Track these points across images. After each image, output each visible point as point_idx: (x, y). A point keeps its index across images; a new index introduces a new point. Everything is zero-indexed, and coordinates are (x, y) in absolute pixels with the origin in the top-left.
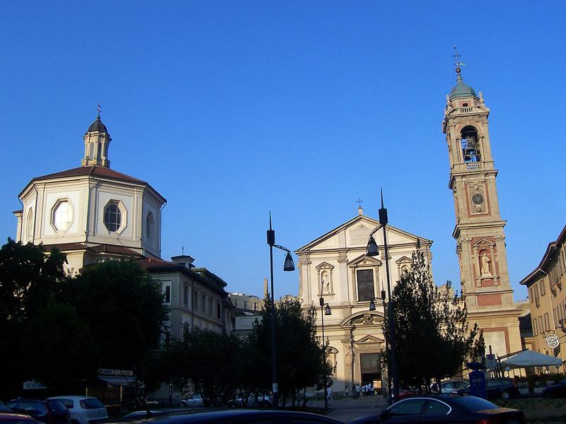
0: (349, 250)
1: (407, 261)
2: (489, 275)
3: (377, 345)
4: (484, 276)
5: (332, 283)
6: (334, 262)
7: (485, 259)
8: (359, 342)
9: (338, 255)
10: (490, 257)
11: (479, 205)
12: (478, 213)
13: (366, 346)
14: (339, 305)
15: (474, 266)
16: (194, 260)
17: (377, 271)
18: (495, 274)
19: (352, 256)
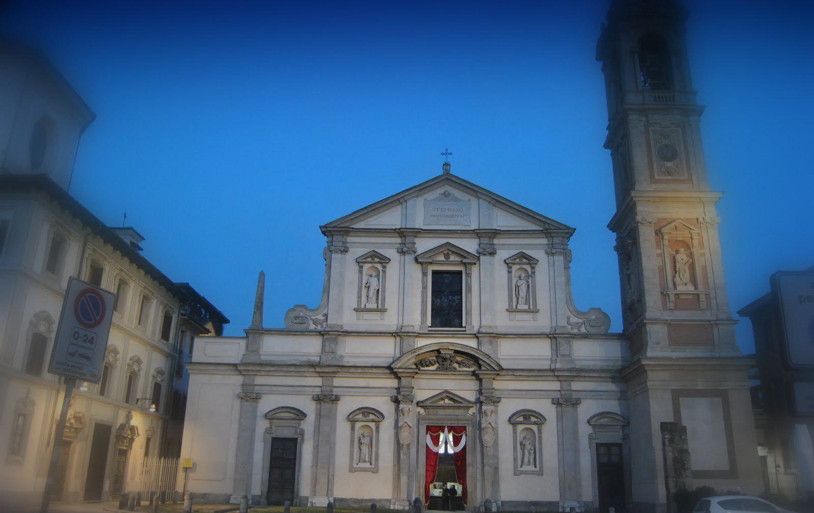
0: (418, 232)
1: (524, 260)
2: (690, 288)
3: (459, 412)
4: (680, 288)
5: (384, 291)
6: (391, 253)
7: (682, 257)
8: (428, 403)
9: (399, 240)
10: (691, 255)
11: (669, 164)
12: (669, 178)
13: (441, 412)
14: (394, 329)
15: (662, 270)
16: (143, 239)
17: (469, 275)
18: (700, 287)
19: (424, 245)
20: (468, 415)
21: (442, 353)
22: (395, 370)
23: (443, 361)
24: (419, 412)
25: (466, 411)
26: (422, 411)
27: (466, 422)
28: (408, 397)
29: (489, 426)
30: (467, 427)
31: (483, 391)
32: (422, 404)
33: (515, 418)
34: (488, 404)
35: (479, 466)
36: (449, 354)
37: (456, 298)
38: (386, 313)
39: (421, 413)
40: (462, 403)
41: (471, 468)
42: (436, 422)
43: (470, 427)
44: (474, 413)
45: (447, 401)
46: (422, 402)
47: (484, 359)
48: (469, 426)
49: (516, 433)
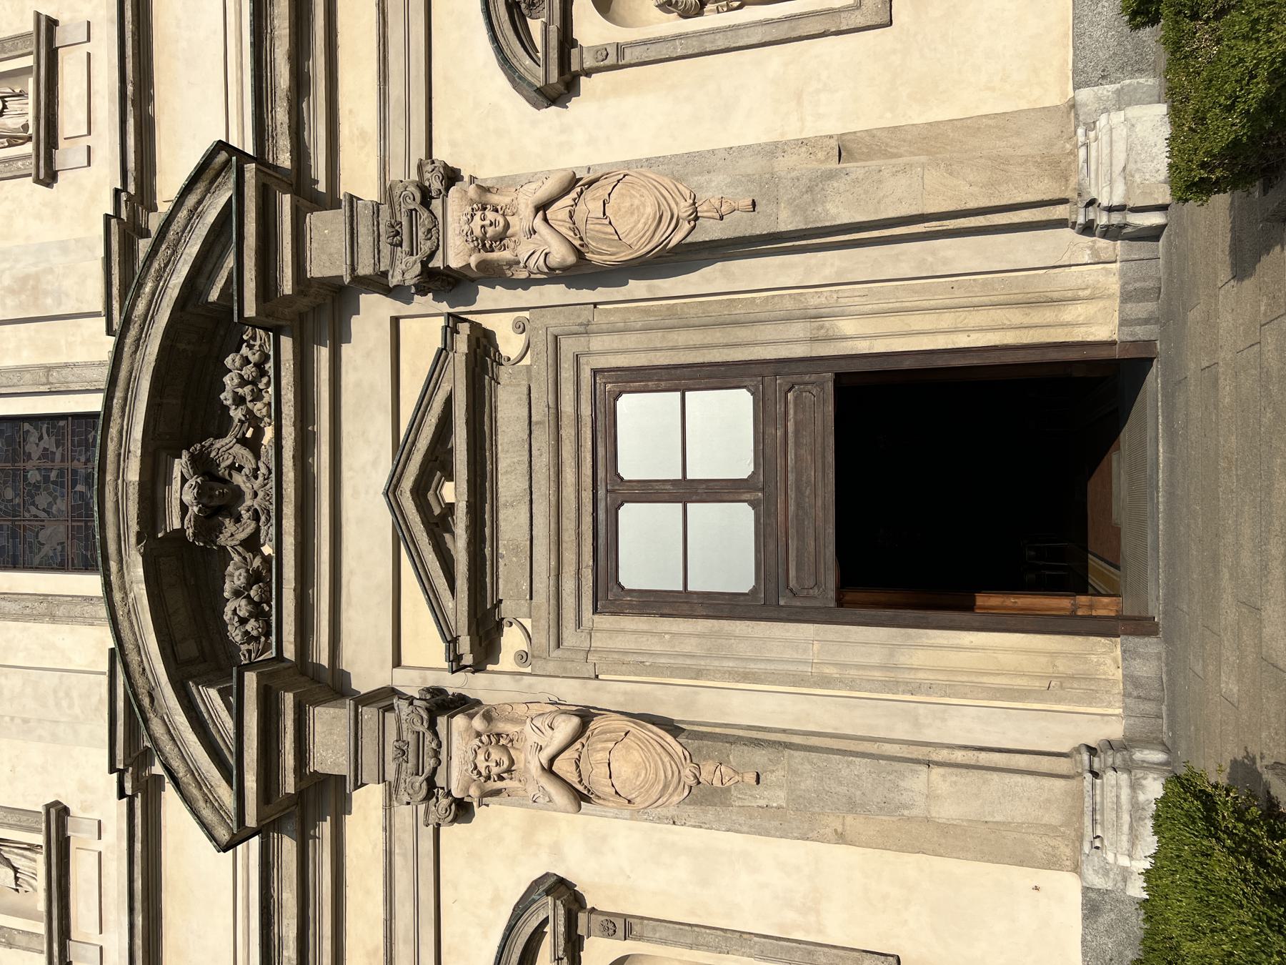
8: (458, 607)
20: (527, 361)
21: (177, 525)
22: (251, 821)
23: (238, 519)
24: (523, 657)
25: (504, 373)
26: (512, 640)
27: (567, 374)
28: (409, 737)
29: (558, 212)
30: (602, 363)
31: (365, 269)
32: (465, 644)
33: (528, 62)
34: (436, 229)
35: (827, 265)
36: (184, 480)
37: (34, 448)
38: (74, 810)
39: (524, 646)
40: (449, 402)
41: (847, 326)
42: (569, 556)
43: (597, 343)
44: (520, 327)
45: (452, 492)
46: (452, 642)
47: (183, 270)
48: (589, 353)
49: (620, 48)
